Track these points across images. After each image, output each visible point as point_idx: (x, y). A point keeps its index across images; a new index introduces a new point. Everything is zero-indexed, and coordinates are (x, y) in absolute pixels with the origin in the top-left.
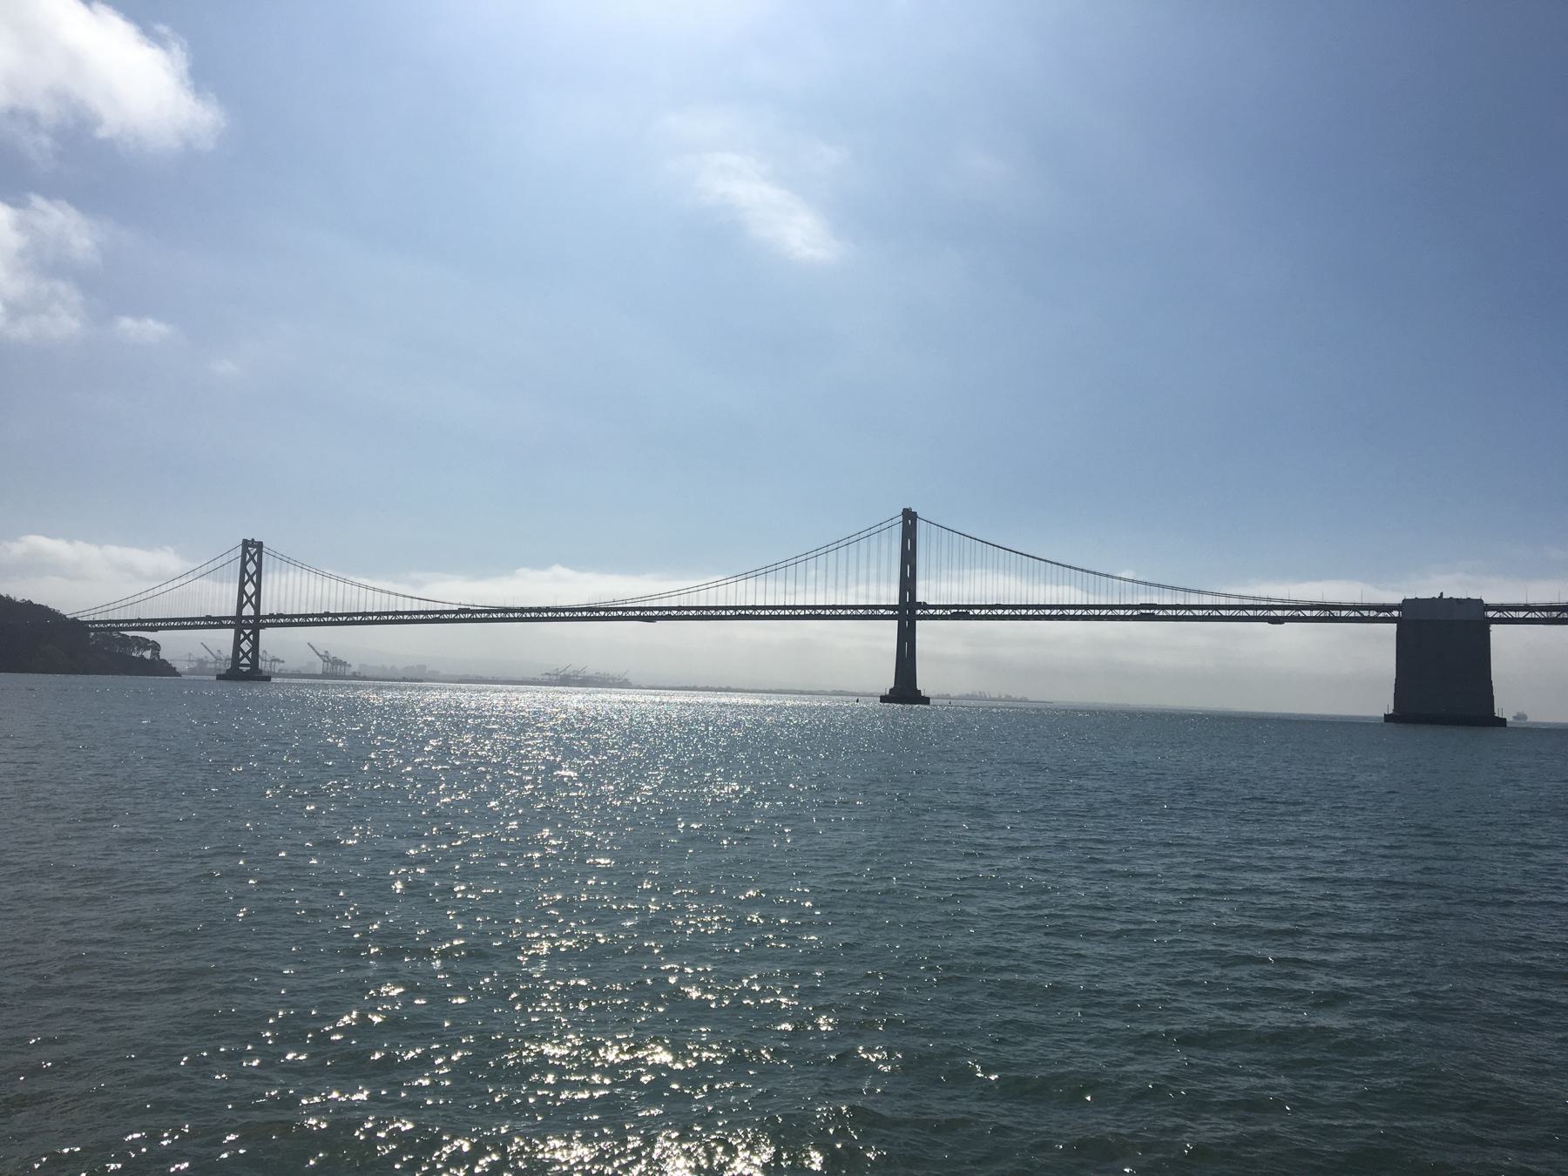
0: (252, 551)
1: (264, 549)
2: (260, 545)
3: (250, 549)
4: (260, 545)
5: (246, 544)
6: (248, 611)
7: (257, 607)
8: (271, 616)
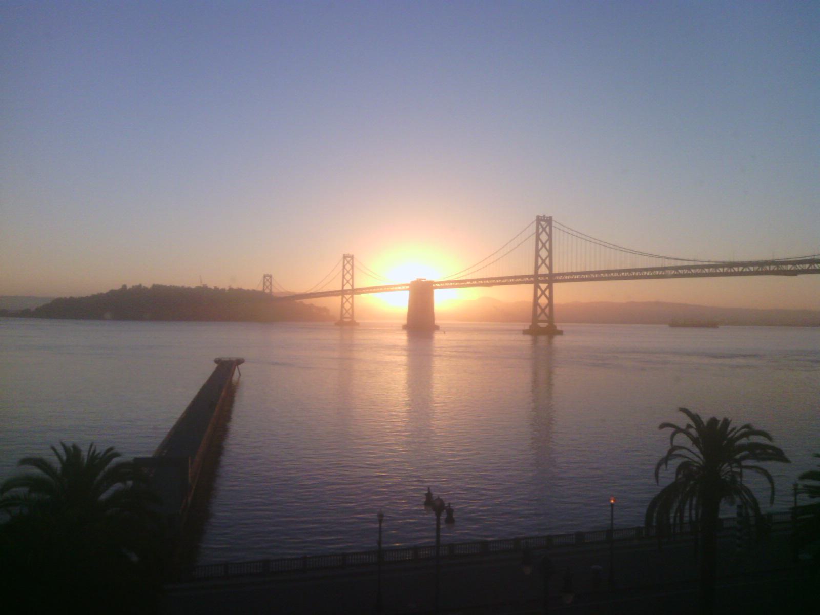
0: (544, 223)
1: (554, 224)
2: (549, 221)
3: (543, 223)
4: (551, 218)
5: (539, 220)
6: (543, 270)
7: (550, 268)
8: (559, 274)
